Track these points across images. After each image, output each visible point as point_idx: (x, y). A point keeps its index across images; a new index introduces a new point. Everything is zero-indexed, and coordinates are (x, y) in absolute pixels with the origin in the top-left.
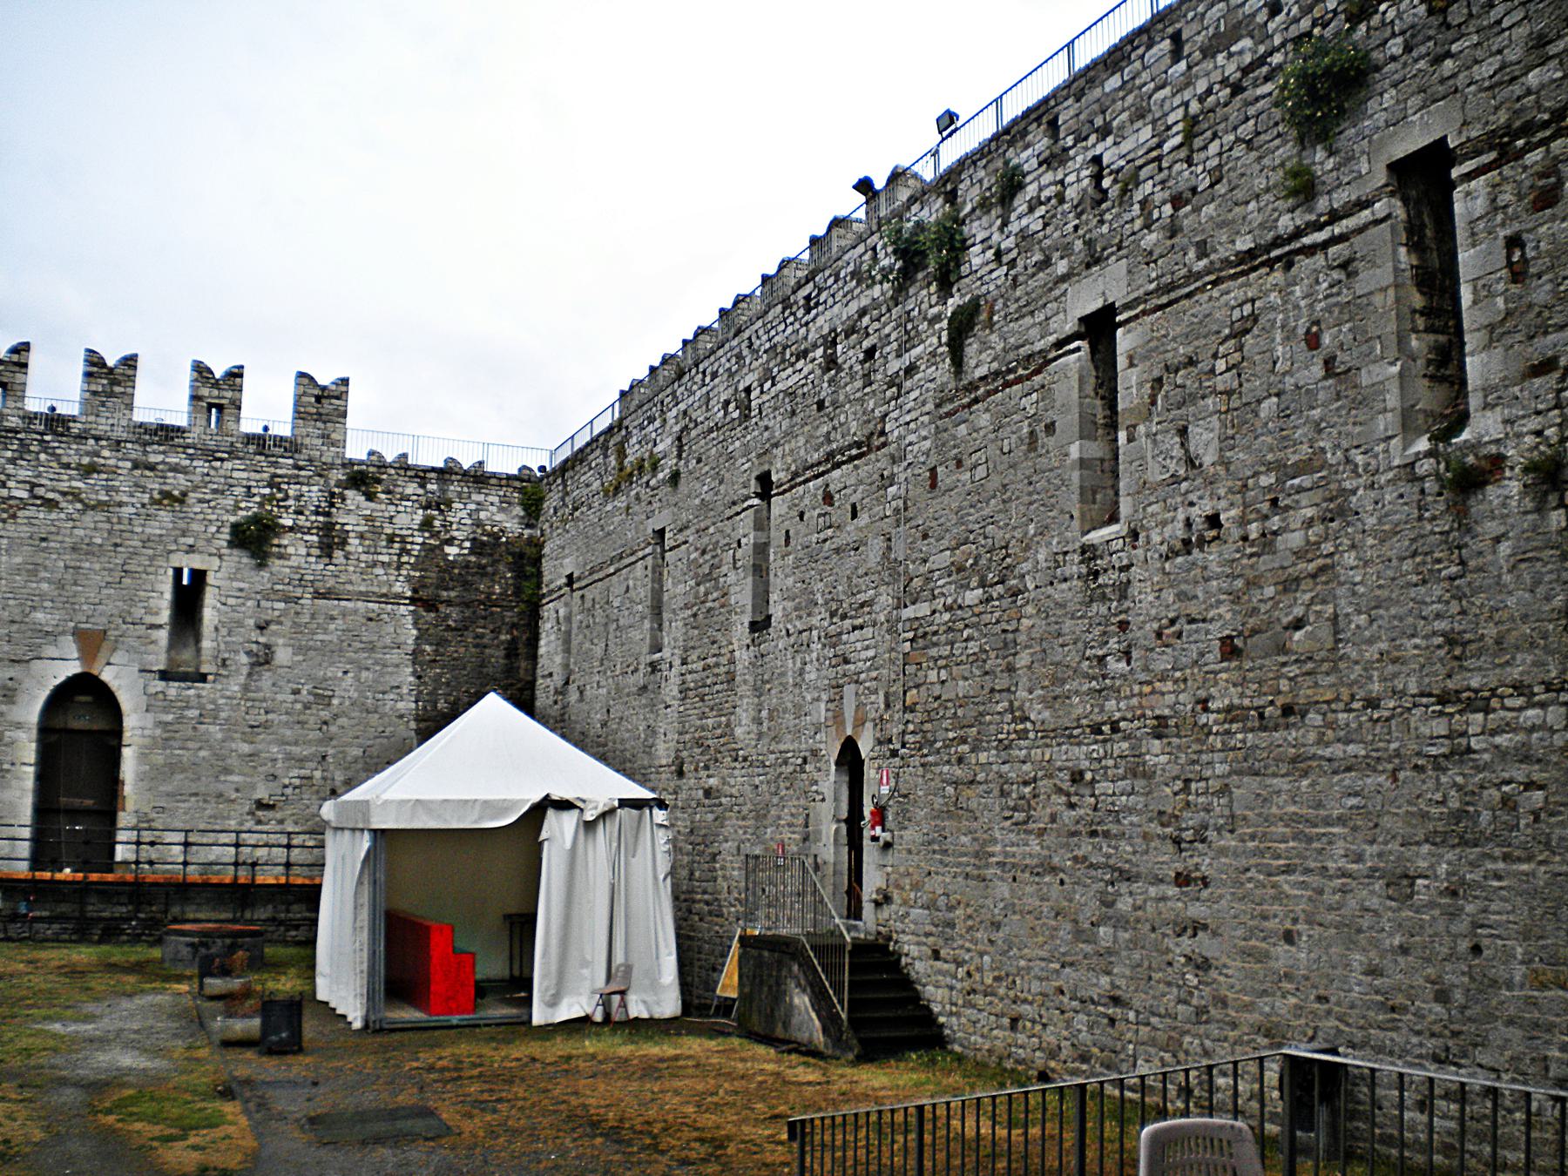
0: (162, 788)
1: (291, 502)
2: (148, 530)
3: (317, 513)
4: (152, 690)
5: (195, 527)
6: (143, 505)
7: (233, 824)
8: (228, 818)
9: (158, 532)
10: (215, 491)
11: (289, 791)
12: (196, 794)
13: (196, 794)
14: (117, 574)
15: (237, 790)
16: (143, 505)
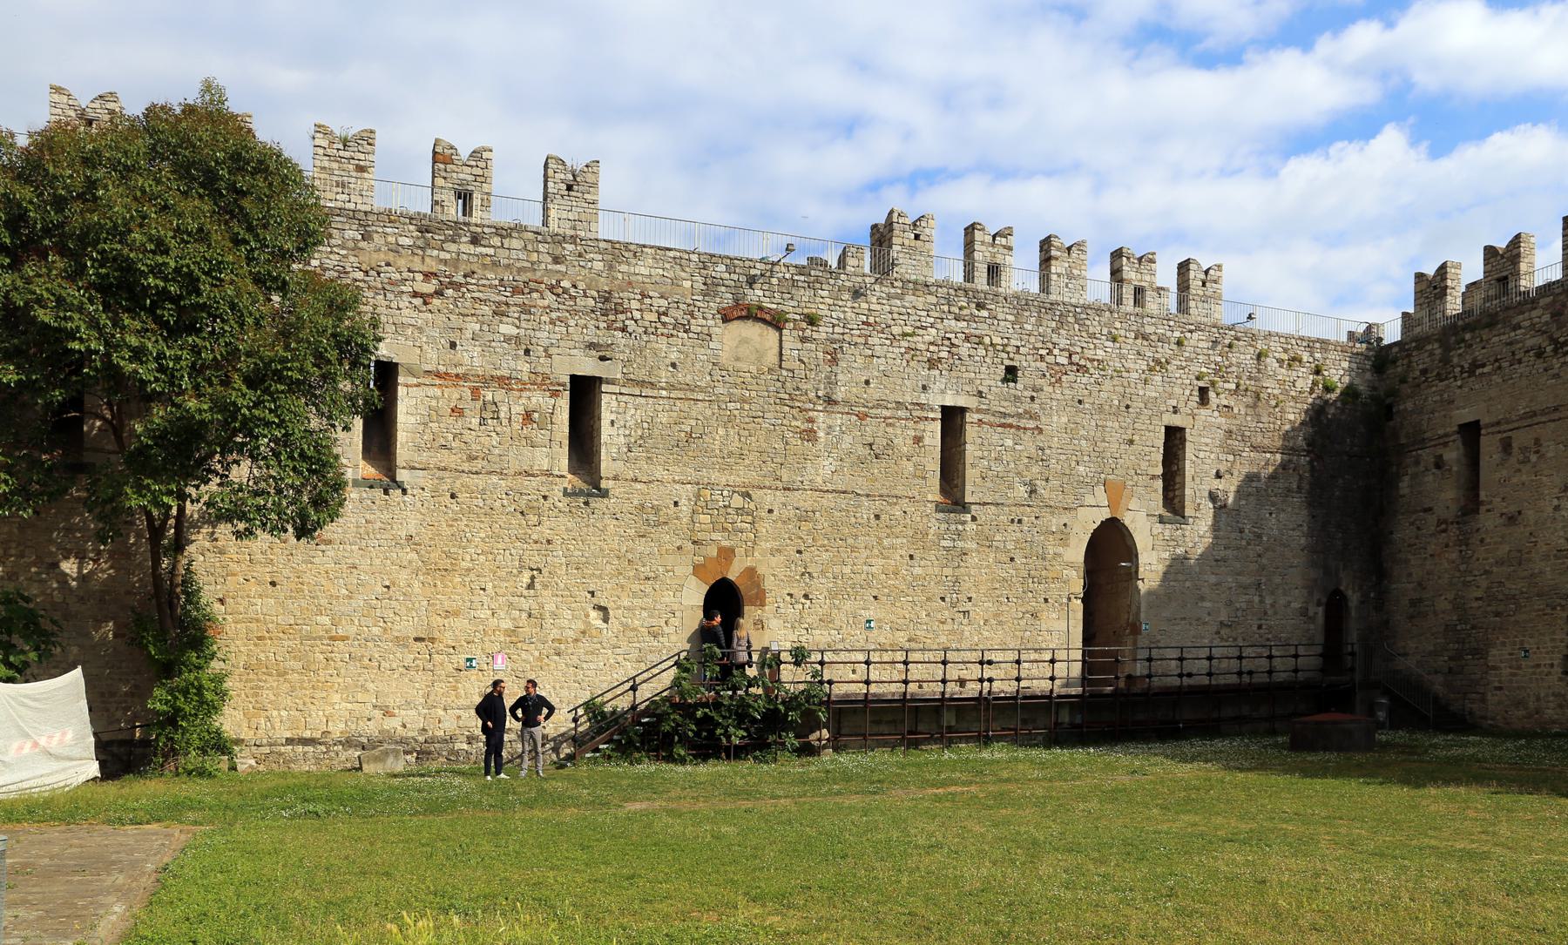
0: (1164, 615)
1: (1234, 369)
2: (1148, 393)
3: (1250, 378)
4: (1155, 532)
5: (1177, 390)
6: (1144, 372)
7: (1206, 641)
8: (1203, 638)
9: (1154, 394)
10: (1188, 359)
11: (1239, 613)
12: (1185, 618)
13: (1185, 618)
14: (1130, 432)
15: (1209, 614)
16: (1144, 372)
